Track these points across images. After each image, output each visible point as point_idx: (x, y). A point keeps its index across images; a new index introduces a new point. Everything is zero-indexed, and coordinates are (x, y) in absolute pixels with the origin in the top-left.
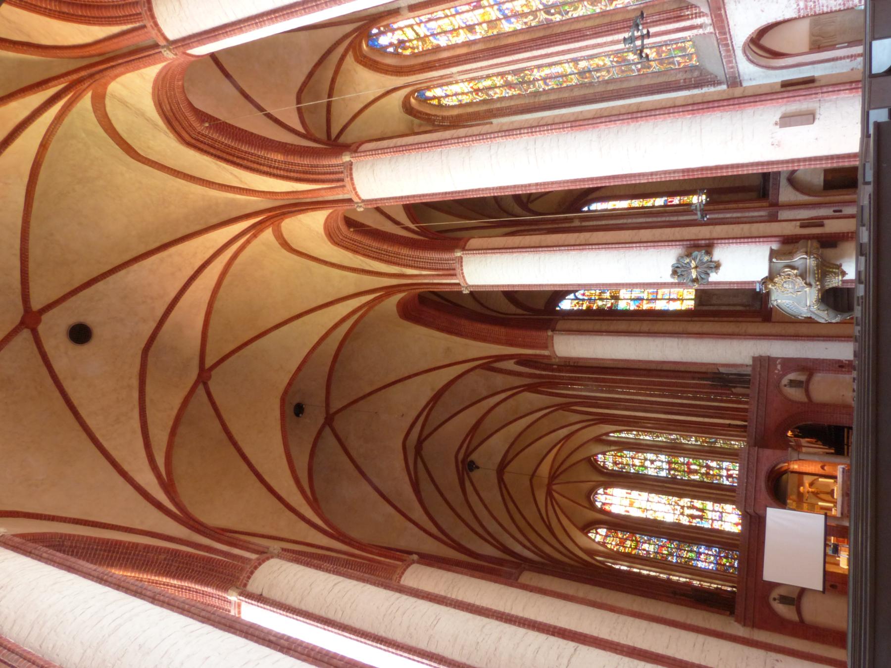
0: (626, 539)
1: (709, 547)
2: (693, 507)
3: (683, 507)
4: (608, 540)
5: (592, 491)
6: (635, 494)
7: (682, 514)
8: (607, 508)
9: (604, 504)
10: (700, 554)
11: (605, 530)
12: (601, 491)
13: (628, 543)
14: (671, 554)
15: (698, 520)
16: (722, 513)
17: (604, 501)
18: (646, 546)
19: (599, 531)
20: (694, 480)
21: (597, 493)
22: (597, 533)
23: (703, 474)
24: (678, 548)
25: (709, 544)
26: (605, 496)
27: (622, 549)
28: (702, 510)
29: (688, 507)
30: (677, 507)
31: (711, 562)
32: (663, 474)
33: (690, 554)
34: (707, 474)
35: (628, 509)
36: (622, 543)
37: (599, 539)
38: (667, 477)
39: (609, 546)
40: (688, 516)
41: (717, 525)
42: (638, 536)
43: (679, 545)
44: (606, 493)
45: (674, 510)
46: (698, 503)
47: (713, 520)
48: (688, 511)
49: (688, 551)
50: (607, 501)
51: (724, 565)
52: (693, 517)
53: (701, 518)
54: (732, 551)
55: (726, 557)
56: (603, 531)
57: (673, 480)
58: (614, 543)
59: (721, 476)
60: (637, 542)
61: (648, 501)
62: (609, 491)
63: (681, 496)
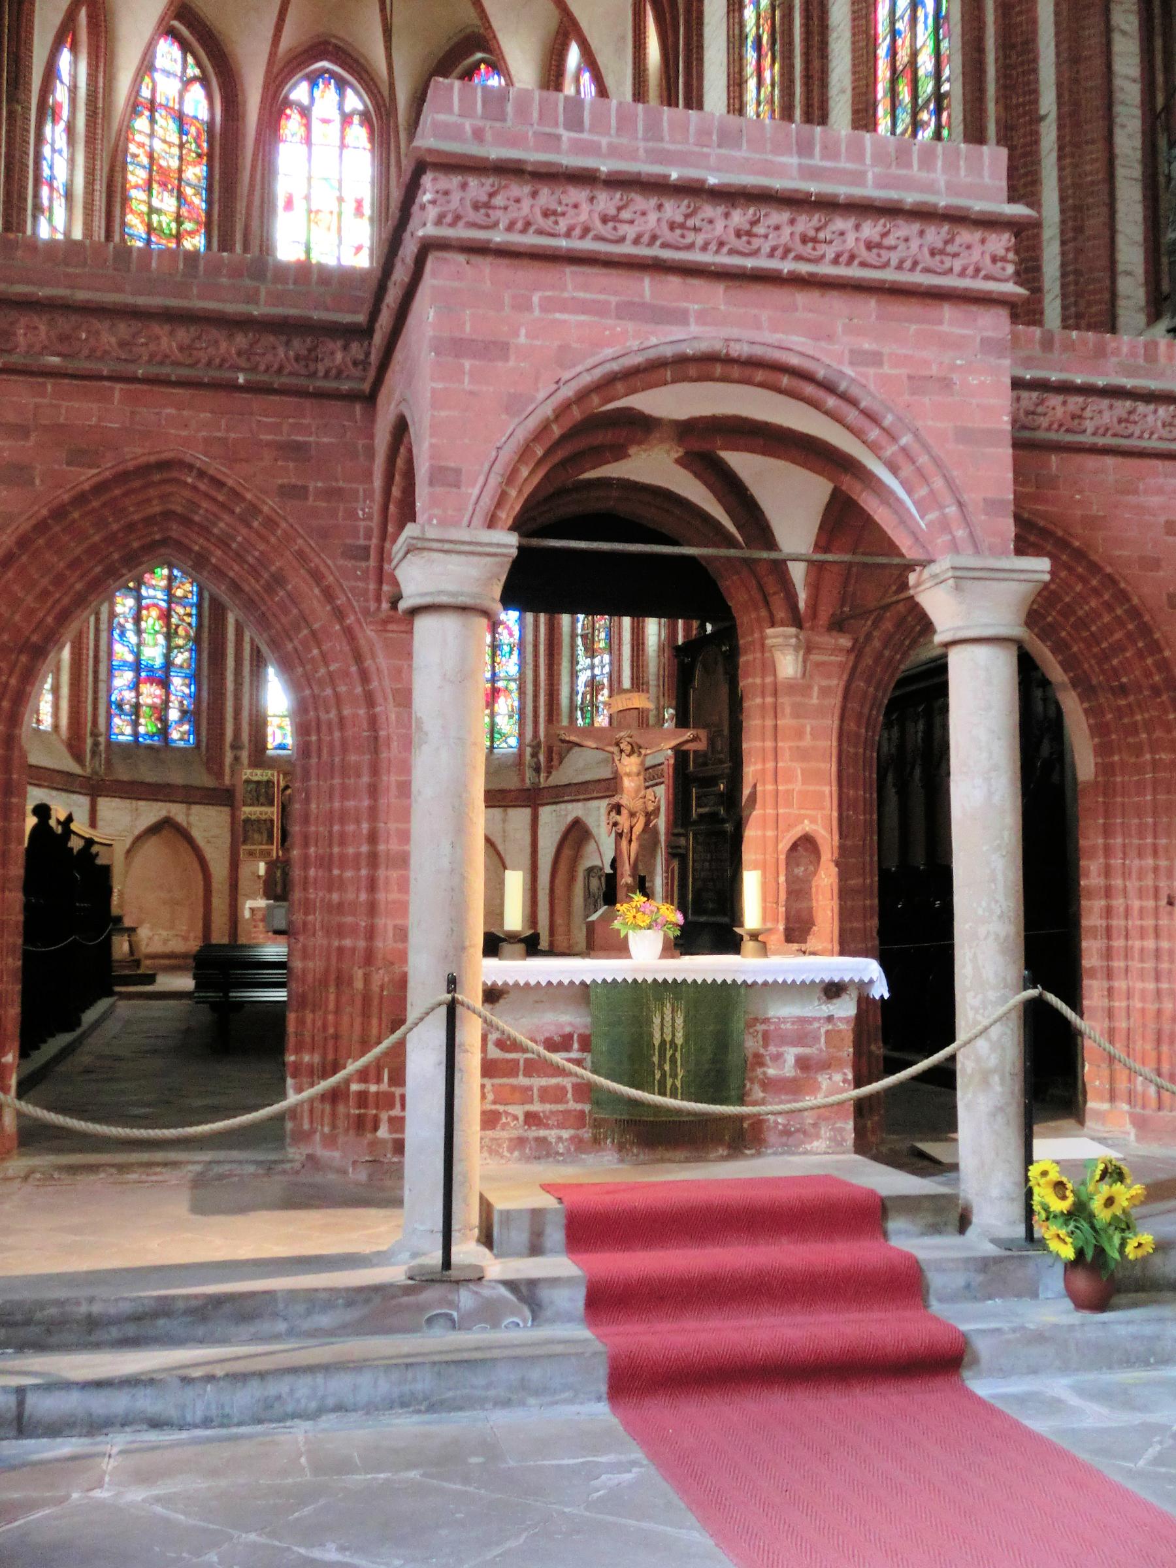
0: (180, 196)
4: (167, 127)
5: (353, 66)
8: (292, 126)
9: (305, 112)
11: (204, 115)
12: (353, 102)
13: (167, 203)
17: (317, 113)
19: (197, 90)
21: (341, 85)
22: (187, 83)
26: (336, 117)
27: (136, 175)
35: (299, 204)
36: (157, 177)
37: (167, 88)
39: (141, 123)
44: (346, 120)
50: (316, 125)
56: (197, 104)
58: (158, 146)
62: (358, 134)
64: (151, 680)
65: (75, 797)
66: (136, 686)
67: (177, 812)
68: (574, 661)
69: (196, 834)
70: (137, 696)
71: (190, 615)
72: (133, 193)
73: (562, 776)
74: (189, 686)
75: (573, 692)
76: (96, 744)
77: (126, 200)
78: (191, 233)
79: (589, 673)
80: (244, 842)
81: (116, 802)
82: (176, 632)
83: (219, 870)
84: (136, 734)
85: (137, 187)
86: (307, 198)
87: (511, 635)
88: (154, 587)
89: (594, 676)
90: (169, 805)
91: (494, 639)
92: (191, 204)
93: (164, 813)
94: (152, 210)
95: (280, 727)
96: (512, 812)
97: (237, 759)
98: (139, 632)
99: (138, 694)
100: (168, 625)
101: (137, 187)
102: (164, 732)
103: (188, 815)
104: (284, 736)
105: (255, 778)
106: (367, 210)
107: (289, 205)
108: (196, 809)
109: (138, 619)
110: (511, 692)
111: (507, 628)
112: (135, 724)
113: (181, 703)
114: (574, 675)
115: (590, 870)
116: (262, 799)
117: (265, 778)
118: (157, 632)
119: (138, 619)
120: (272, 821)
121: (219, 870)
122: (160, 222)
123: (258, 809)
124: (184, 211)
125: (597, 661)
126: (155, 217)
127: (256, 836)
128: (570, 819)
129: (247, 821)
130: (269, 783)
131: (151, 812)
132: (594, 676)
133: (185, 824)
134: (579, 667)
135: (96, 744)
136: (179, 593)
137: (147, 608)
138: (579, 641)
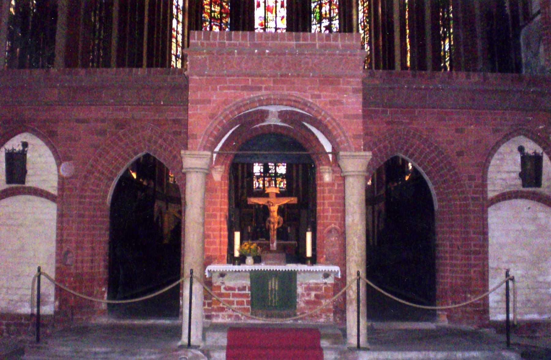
6: (283, 12)
42: (228, 20)
60: (221, 19)
72: (206, 6)
77: (203, 8)
78: (225, 18)
85: (207, 4)
86: (265, 2)
92: (225, 8)
94: (212, 11)
101: (207, 4)
104: (259, 184)
106: (285, 5)
107: (259, 6)
122: (214, 15)
124: (223, 11)
126: (213, 14)
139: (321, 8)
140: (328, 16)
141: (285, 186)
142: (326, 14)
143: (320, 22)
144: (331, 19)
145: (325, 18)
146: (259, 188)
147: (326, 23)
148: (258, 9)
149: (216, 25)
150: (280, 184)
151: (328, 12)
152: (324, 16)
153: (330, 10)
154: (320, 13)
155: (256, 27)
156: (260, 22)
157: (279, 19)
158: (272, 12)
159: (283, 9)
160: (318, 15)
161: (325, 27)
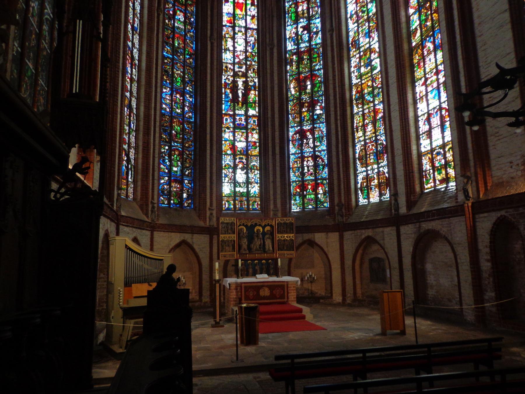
1: (194, 108)
2: (247, 89)
3: (245, 75)
6: (253, 11)
7: (236, 75)
10: (183, 95)
14: (175, 51)
15: (230, 95)
16: (246, 128)
18: (180, 16)
20: (288, 89)
23: (299, 98)
24: (184, 64)
25: (199, 108)
28: (245, 102)
29: (246, 83)
30: (244, 67)
31: (171, 108)
32: (290, 46)
33: (179, 79)
34: (301, 105)
38: (286, 52)
40: (235, 82)
41: (227, 121)
43: (190, 65)
45: (239, 63)
46: (253, 95)
47: (234, 116)
48: (240, 82)
49: (183, 78)
51: (172, 128)
52: (234, 88)
53: (235, 99)
54: (195, 141)
55: (183, 129)
57: (283, 61)
59: (301, 124)
61: (247, 28)
63: (260, 73)
64: (176, 181)
65: (144, 231)
66: (169, 183)
67: (187, 237)
68: (355, 169)
69: (196, 247)
70: (170, 188)
71: (191, 155)
73: (353, 219)
74: (191, 184)
75: (356, 183)
76: (153, 207)
78: (191, 5)
79: (365, 173)
80: (222, 251)
81: (162, 234)
82: (186, 162)
83: (205, 262)
84: (169, 203)
87: (323, 161)
88: (177, 142)
89: (368, 175)
90: (184, 234)
91: (315, 163)
93: (182, 238)
95: (228, 201)
96: (330, 234)
97: (211, 214)
98: (170, 161)
99: (170, 187)
100: (182, 158)
102: (181, 203)
103: (192, 238)
104: (229, 205)
105: (226, 221)
108: (196, 236)
109: (170, 155)
110: (324, 184)
111: (321, 158)
112: (169, 200)
113: (188, 191)
114: (356, 176)
115: (372, 260)
116: (229, 231)
117: (231, 222)
118: (179, 161)
119: (170, 155)
120: (234, 241)
121: (205, 262)
123: (228, 236)
125: (369, 168)
127: (227, 248)
128: (363, 237)
129: (223, 241)
130: (232, 224)
131: (176, 238)
132: (368, 175)
133: (191, 243)
134: (358, 172)
135: (153, 207)
136: (187, 145)
137: (174, 150)
138: (358, 162)
139: (297, 7)
140: (306, 15)
141: (259, 207)
142: (303, 14)
143: (296, 22)
144: (309, 19)
145: (303, 18)
146: (228, 209)
147: (303, 22)
148: (226, 4)
149: (181, 11)
150: (253, 205)
151: (305, 11)
152: (301, 16)
153: (308, 9)
154: (296, 12)
155: (224, 24)
156: (229, 19)
157: (249, 18)
158: (241, 10)
159: (253, 7)
160: (293, 15)
161: (301, 27)
